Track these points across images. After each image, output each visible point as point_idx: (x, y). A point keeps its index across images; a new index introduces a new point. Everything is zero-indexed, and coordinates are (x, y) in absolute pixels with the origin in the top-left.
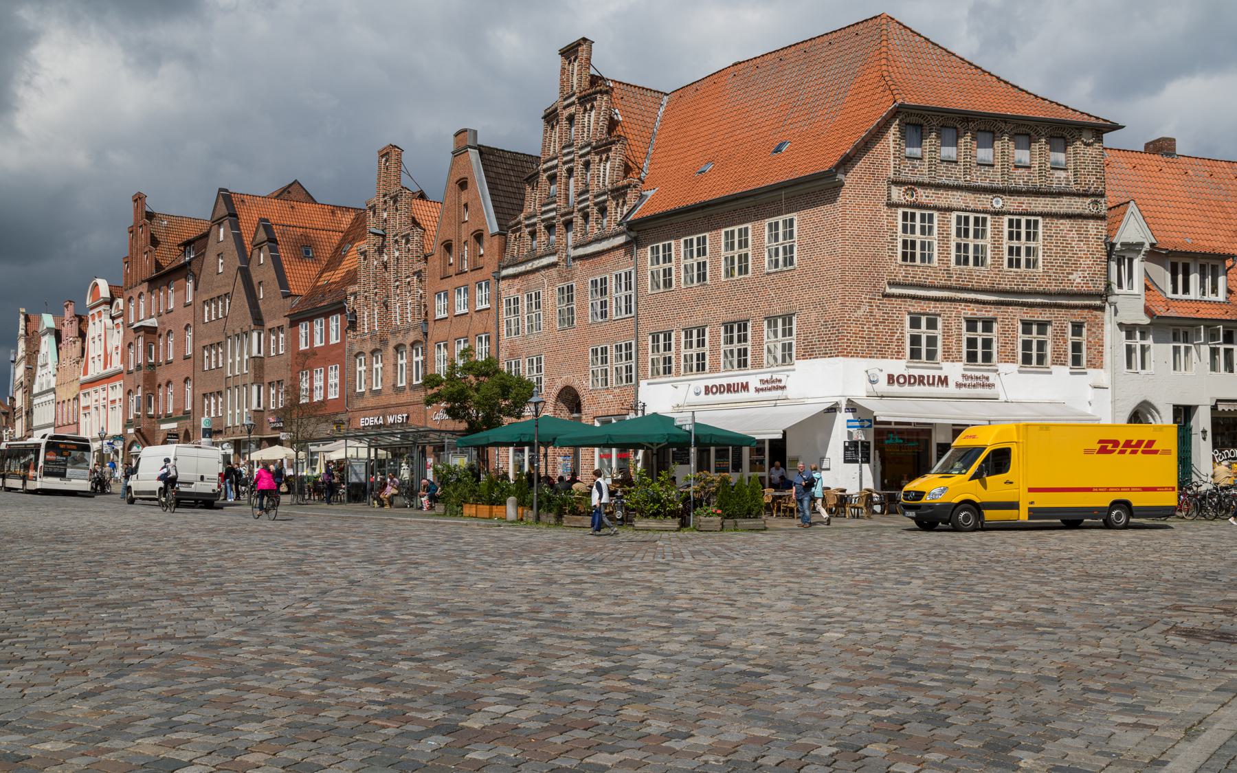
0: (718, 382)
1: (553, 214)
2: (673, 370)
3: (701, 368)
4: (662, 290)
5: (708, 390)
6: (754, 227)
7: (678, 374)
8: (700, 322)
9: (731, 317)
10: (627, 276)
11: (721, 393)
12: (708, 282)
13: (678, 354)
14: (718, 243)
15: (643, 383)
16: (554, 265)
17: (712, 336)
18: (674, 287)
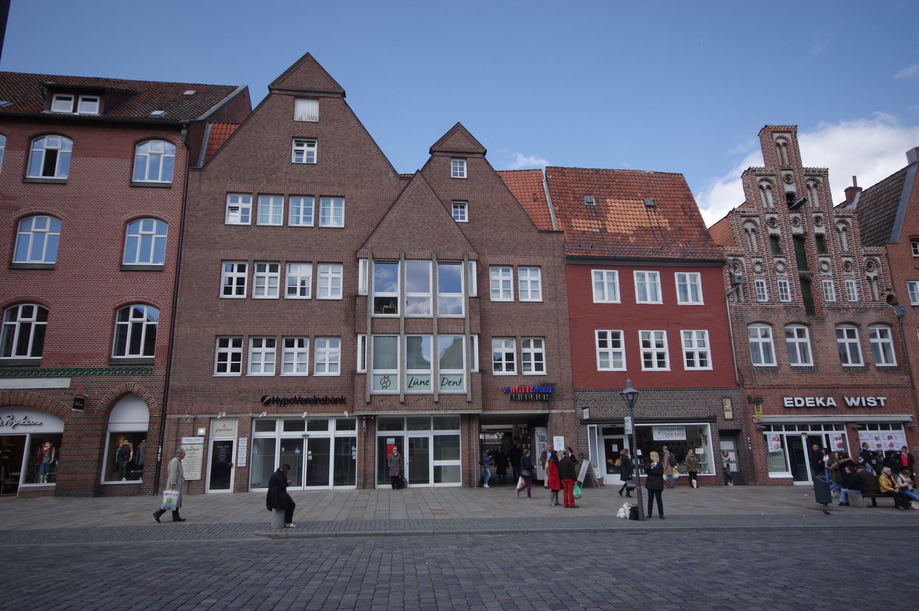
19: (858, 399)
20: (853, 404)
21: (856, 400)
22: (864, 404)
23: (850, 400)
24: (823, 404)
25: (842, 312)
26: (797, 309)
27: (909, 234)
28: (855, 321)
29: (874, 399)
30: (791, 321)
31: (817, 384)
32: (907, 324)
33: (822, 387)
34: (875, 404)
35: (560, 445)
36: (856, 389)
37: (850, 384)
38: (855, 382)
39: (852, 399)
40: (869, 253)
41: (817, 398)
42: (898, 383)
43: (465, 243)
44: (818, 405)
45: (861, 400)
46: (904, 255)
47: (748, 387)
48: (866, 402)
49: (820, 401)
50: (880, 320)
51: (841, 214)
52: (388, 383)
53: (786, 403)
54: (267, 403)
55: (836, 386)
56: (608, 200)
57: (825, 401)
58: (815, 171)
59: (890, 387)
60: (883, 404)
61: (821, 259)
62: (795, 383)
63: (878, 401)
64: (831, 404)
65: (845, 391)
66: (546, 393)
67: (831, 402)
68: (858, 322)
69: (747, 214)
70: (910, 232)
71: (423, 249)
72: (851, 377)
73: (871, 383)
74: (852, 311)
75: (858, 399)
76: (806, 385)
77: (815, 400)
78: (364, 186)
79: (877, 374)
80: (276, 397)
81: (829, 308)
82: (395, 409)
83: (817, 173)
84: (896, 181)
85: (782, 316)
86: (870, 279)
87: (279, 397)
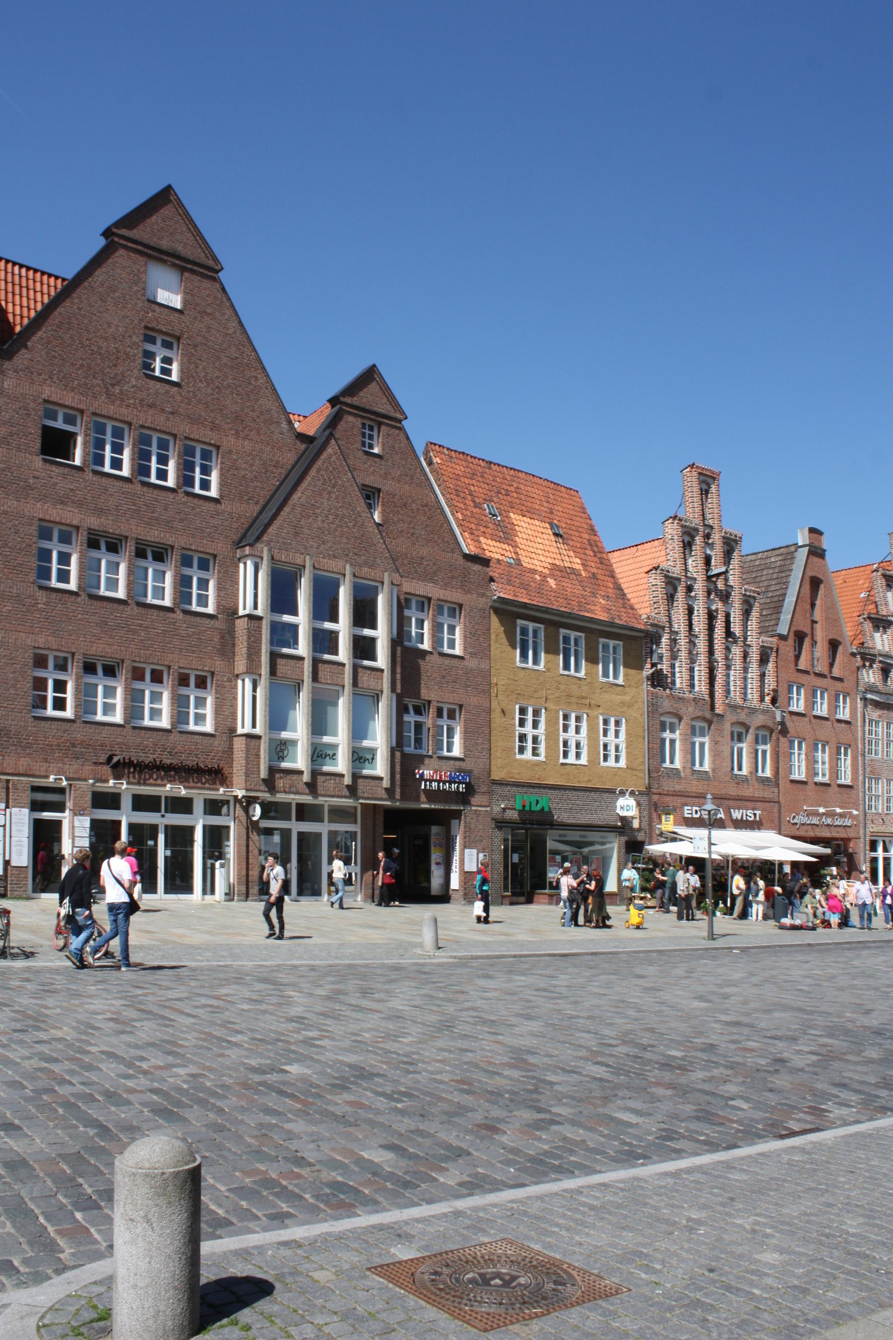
25: (739, 711)
35: (471, 855)
36: (743, 801)
43: (386, 558)
47: (655, 791)
52: (286, 752)
53: (686, 812)
54: (120, 768)
56: (511, 515)
62: (694, 789)
63: (755, 815)
65: (731, 803)
66: (463, 783)
69: (670, 574)
71: (335, 557)
74: (746, 710)
78: (247, 436)
80: (127, 757)
82: (297, 793)
84: (780, 558)
85: (691, 709)
87: (133, 759)
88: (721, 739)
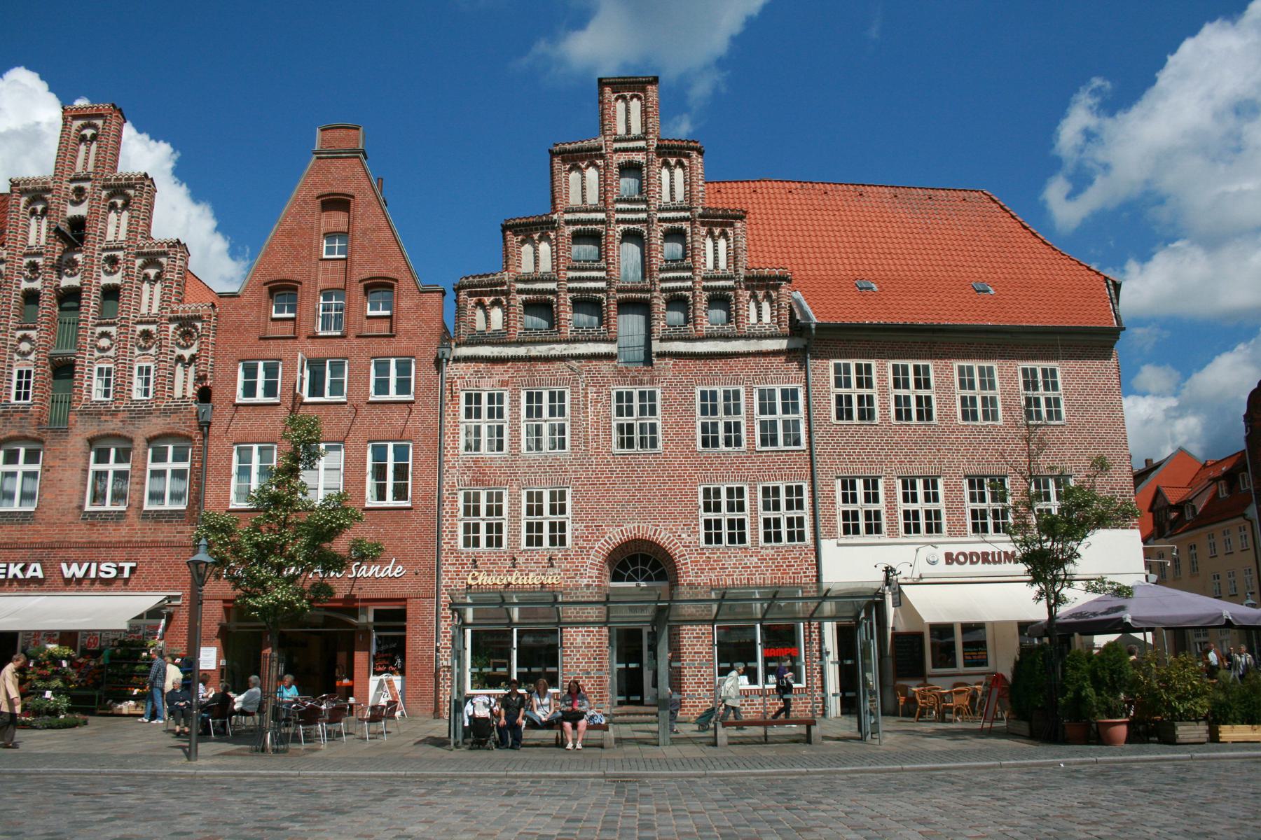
0: (967, 549)
1: (602, 285)
2: (884, 527)
3: (934, 528)
4: (856, 420)
5: (949, 558)
6: (1000, 368)
7: (893, 532)
8: (928, 470)
9: (975, 470)
10: (790, 395)
11: (972, 562)
12: (935, 421)
13: (891, 507)
14: (949, 377)
15: (827, 545)
16: (609, 357)
17: (949, 491)
18: (877, 421)
19: (86, 565)
20: (74, 575)
21: (80, 568)
22: (93, 575)
23: (69, 568)
24: (20, 576)
25: (103, 418)
26: (23, 415)
27: (267, 279)
28: (124, 433)
29: (114, 565)
30: (8, 435)
31: (26, 540)
32: (218, 437)
33: (32, 546)
34: (114, 573)
37: (84, 540)
38: (95, 537)
39: (75, 566)
40: (179, 315)
41: (12, 565)
42: (172, 539)
44: (10, 576)
45: (89, 568)
46: (247, 315)
48: (98, 570)
49: (15, 570)
50: (169, 431)
51: (145, 250)
55: (57, 545)
57: (24, 570)
58: (121, 179)
59: (155, 545)
60: (126, 574)
61: (99, 330)
64: (35, 574)
67: (35, 570)
68: (127, 434)
70: (270, 275)
72: (88, 530)
73: (123, 539)
74: (121, 415)
75: (86, 565)
76: (6, 543)
77: (7, 568)
79: (138, 526)
81: (82, 413)
83: (123, 182)
86: (184, 359)
88: (58, 463)
